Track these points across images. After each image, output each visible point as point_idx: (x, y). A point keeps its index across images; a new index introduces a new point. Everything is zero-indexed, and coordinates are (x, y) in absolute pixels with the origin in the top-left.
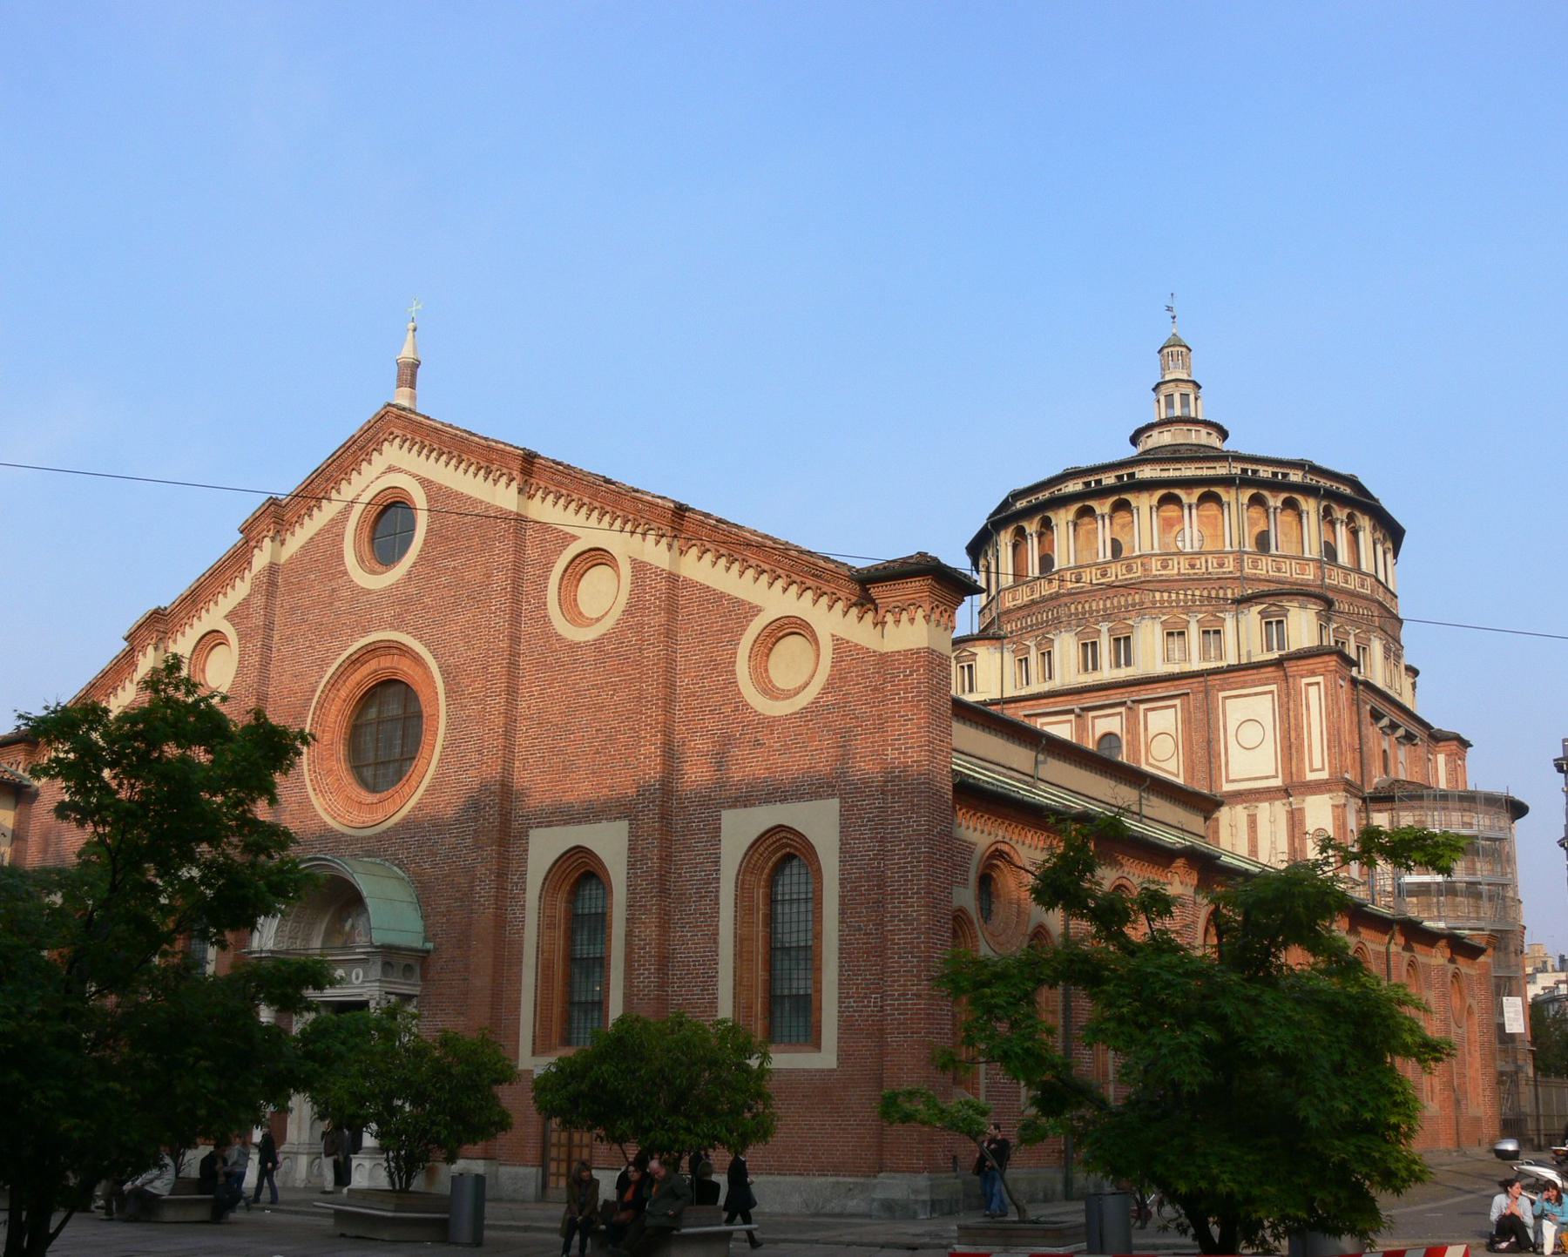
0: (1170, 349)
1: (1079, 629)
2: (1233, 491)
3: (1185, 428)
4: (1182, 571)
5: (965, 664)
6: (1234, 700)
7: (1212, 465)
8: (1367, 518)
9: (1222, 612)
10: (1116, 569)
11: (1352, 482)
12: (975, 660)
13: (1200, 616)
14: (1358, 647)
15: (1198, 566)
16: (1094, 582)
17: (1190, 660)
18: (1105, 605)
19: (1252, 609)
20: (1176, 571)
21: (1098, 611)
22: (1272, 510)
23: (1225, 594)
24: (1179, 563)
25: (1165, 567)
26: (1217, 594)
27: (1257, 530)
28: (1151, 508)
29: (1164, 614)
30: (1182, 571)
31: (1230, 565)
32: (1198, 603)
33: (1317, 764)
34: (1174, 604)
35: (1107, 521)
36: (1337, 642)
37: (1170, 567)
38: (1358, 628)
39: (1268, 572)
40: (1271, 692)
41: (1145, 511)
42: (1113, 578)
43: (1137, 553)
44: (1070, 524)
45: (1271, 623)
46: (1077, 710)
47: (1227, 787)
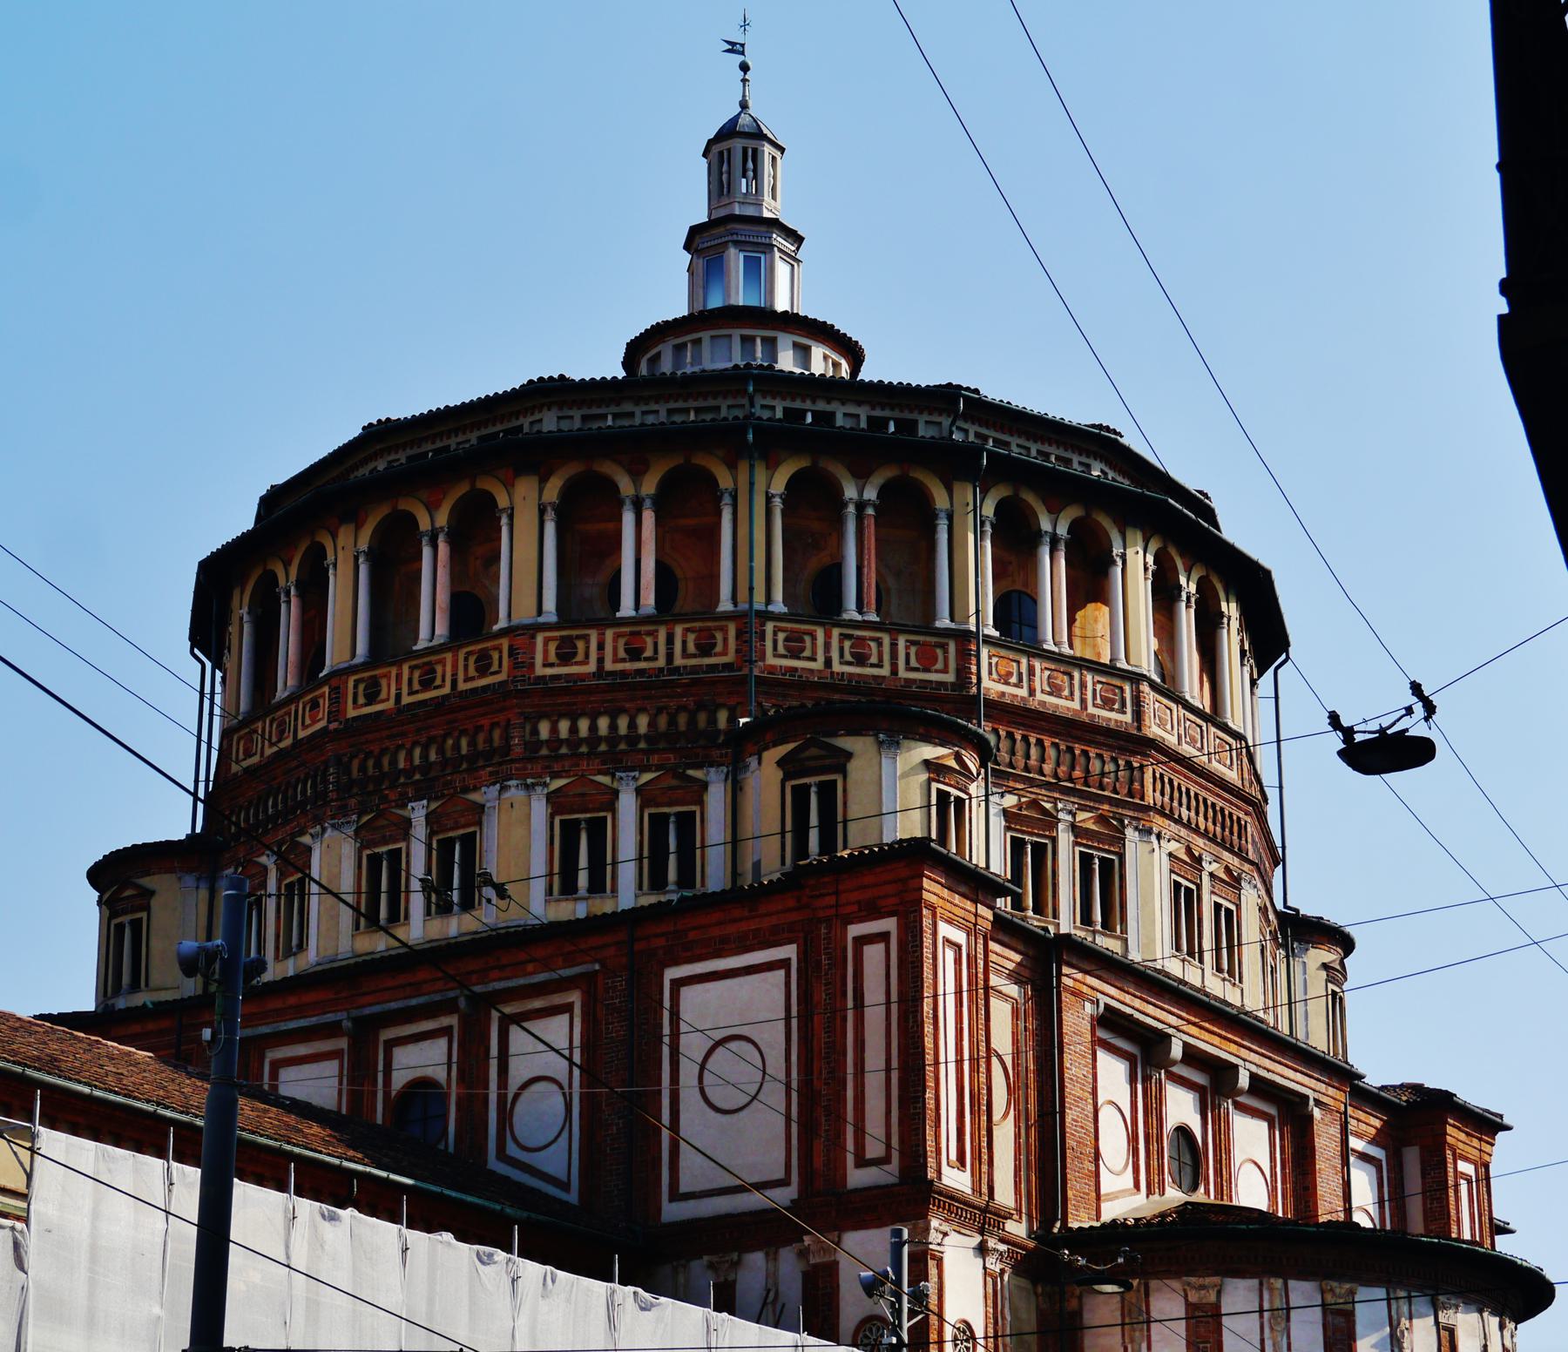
0: (724, 146)
1: (365, 819)
2: (743, 467)
3: (737, 333)
4: (609, 666)
5: (126, 919)
6: (699, 988)
7: (711, 402)
8: (1136, 537)
9: (699, 766)
10: (455, 667)
11: (1101, 442)
12: (148, 909)
13: (647, 777)
14: (1086, 860)
15: (649, 653)
16: (406, 700)
17: (614, 890)
18: (425, 756)
19: (766, 755)
20: (592, 667)
21: (409, 772)
22: (851, 509)
23: (713, 721)
24: (601, 647)
25: (566, 657)
26: (692, 722)
27: (815, 563)
28: (542, 512)
29: (555, 776)
30: (609, 666)
31: (726, 651)
32: (642, 745)
33: (874, 1150)
34: (584, 749)
35: (443, 548)
36: (1017, 846)
37: (580, 657)
38: (1083, 808)
39: (828, 662)
40: (784, 964)
41: (526, 518)
42: (447, 690)
43: (502, 623)
44: (361, 560)
45: (807, 787)
46: (347, 1024)
47: (672, 1212)
